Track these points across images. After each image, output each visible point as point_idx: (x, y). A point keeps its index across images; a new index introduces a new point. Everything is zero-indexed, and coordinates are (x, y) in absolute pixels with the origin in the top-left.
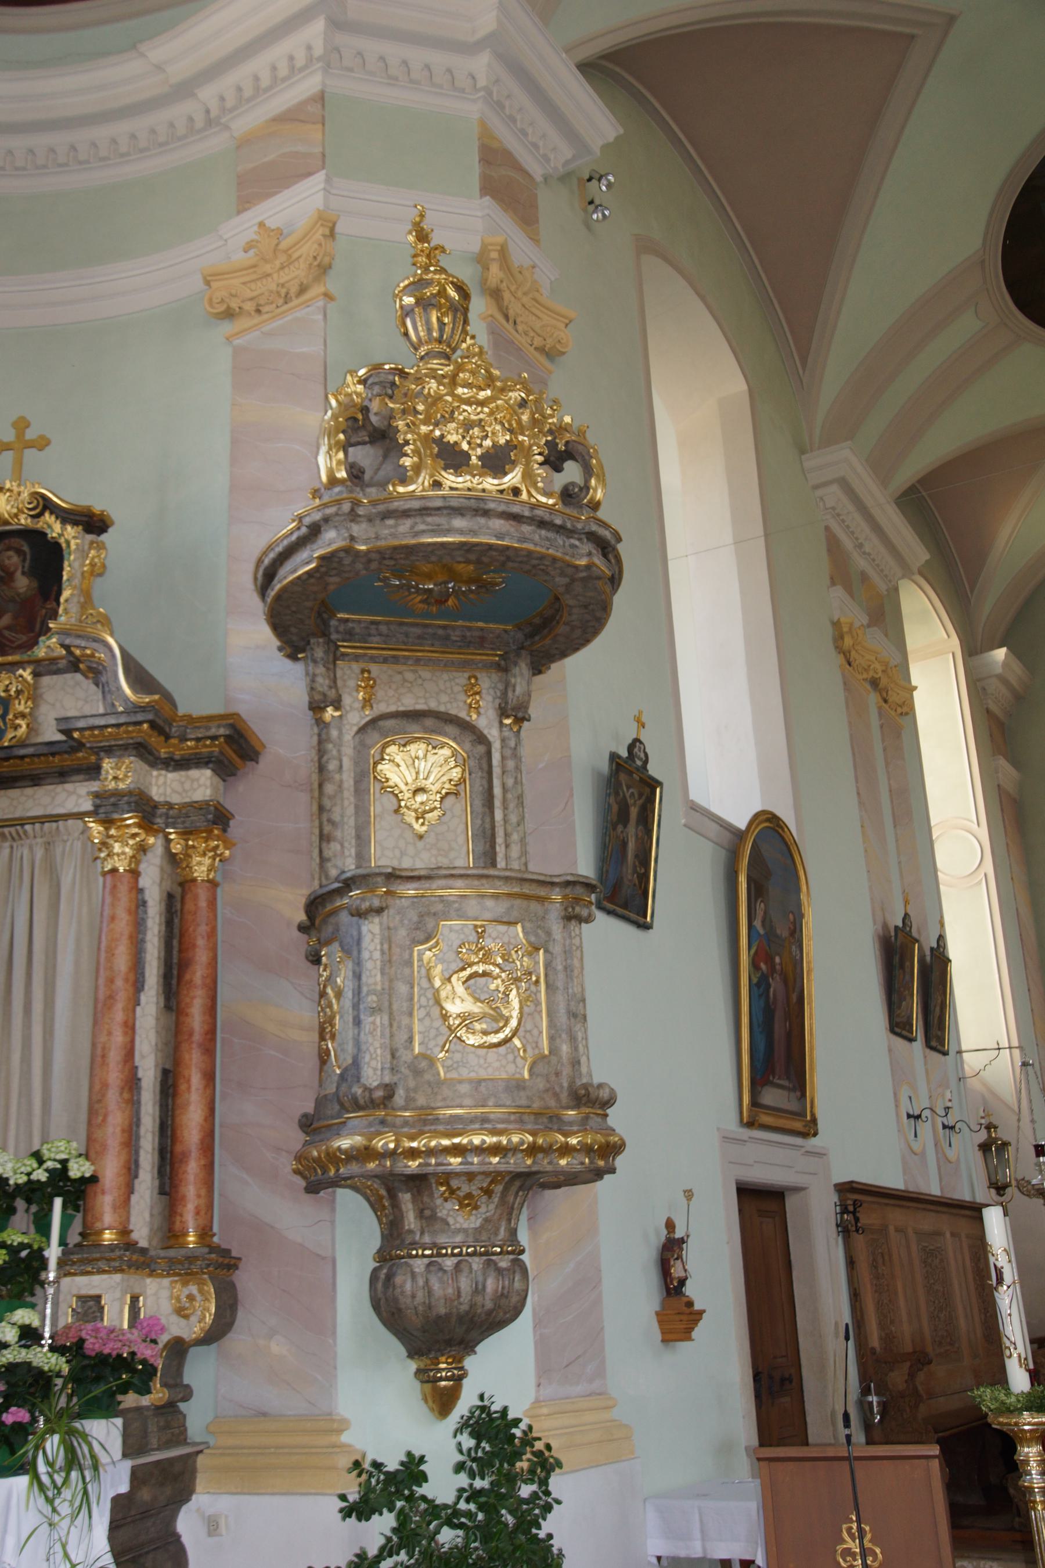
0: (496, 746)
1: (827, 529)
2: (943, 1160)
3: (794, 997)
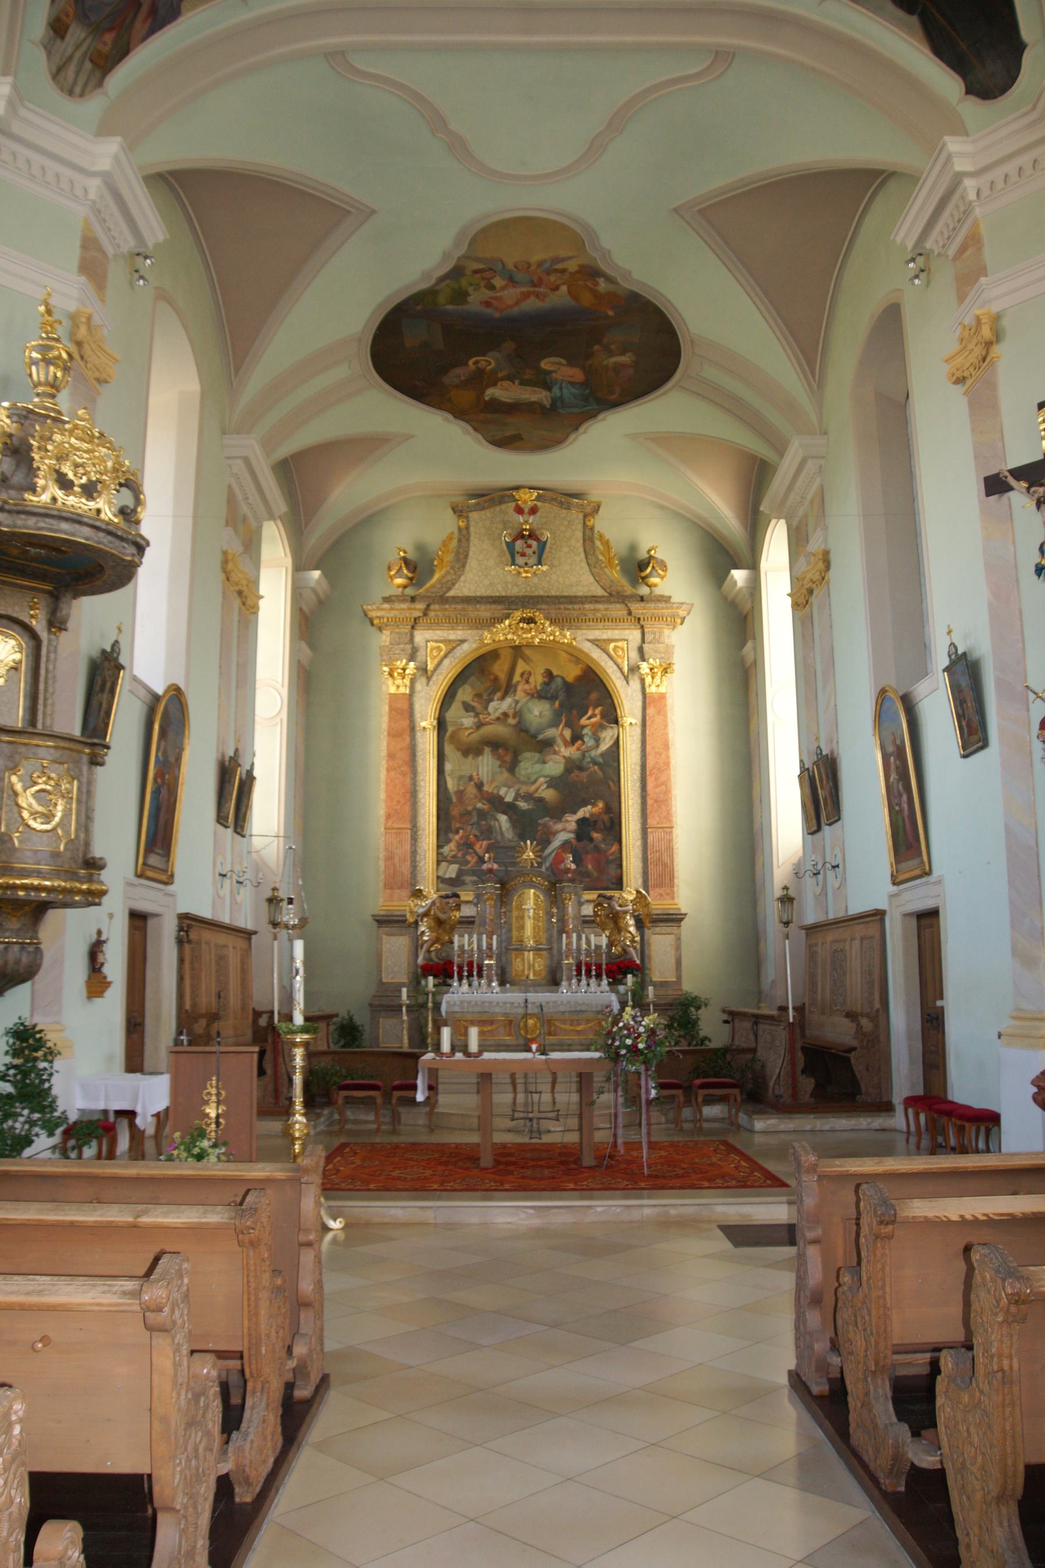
0: (45, 643)
1: (230, 486)
2: (234, 902)
3: (172, 800)
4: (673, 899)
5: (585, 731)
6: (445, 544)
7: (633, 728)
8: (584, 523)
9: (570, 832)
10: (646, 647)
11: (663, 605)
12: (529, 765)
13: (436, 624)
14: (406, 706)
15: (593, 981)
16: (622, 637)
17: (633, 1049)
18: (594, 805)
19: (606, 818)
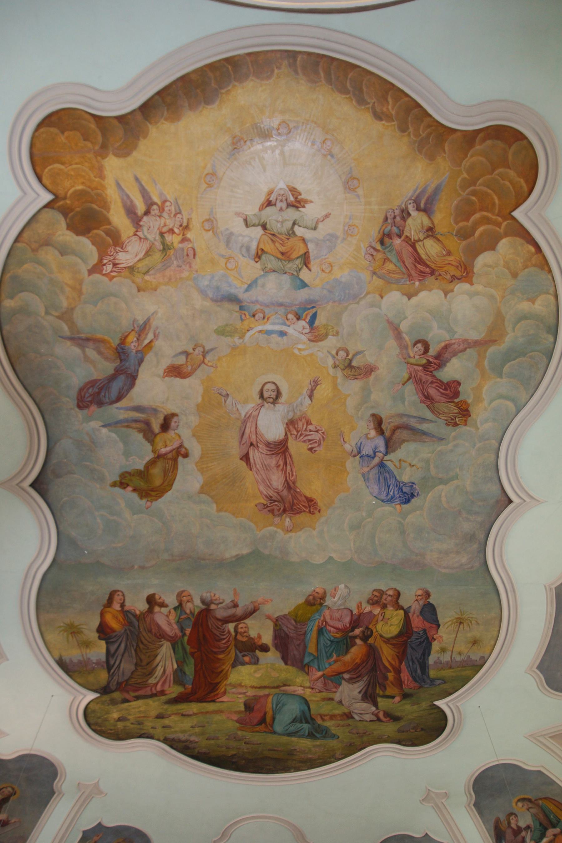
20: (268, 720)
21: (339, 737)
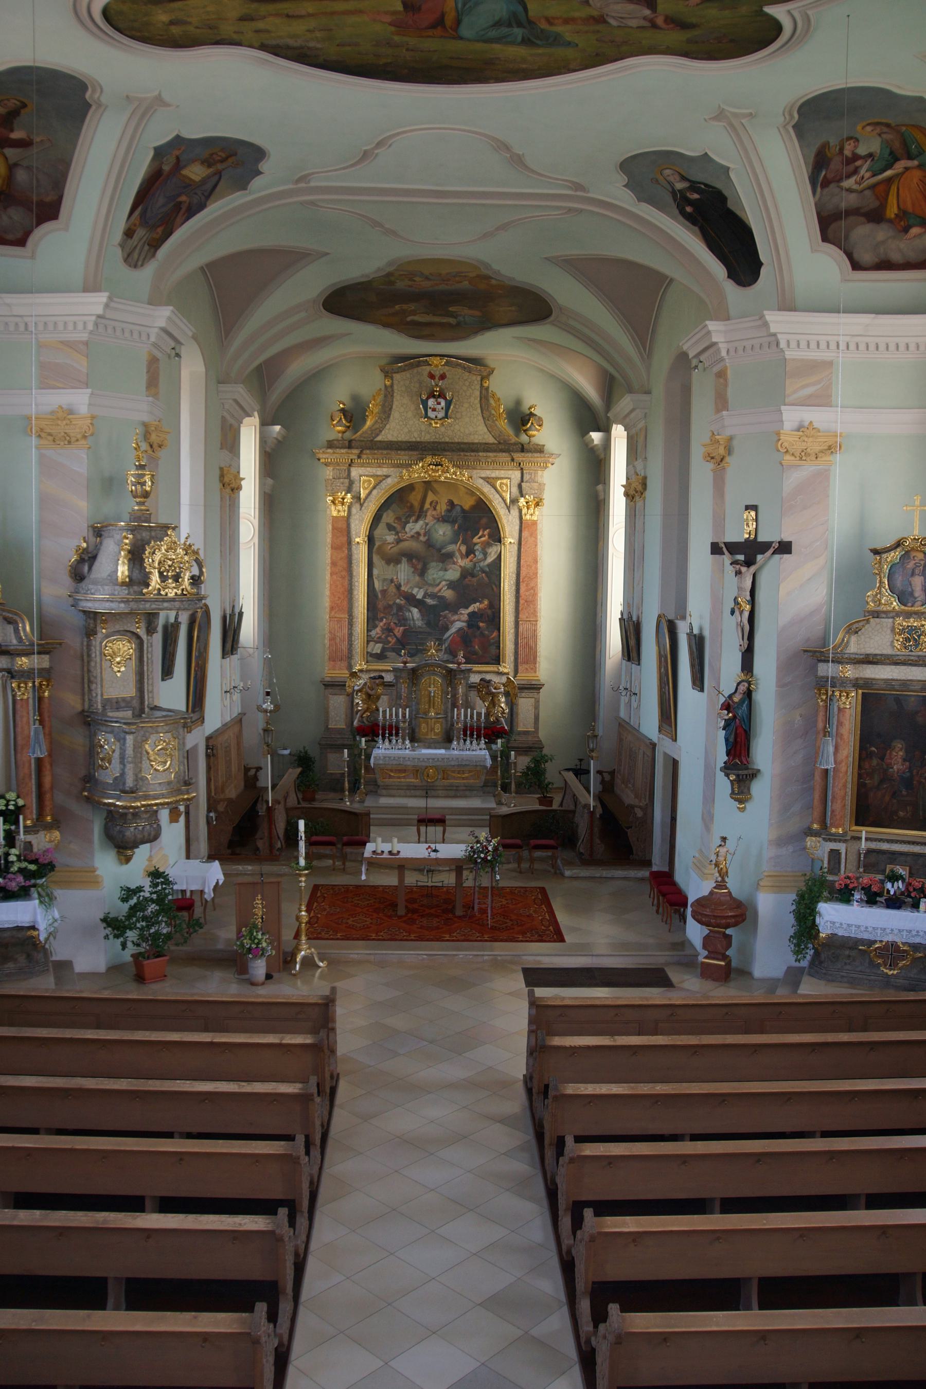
1: (223, 417)
4: (535, 672)
5: (477, 547)
6: (374, 398)
7: (512, 546)
8: (481, 384)
9: (463, 622)
10: (523, 485)
11: (538, 455)
12: (434, 573)
13: (369, 465)
14: (345, 526)
15: (475, 742)
16: (507, 476)
17: (485, 860)
18: (481, 602)
19: (489, 612)
20: (449, 20)
21: (577, 45)
